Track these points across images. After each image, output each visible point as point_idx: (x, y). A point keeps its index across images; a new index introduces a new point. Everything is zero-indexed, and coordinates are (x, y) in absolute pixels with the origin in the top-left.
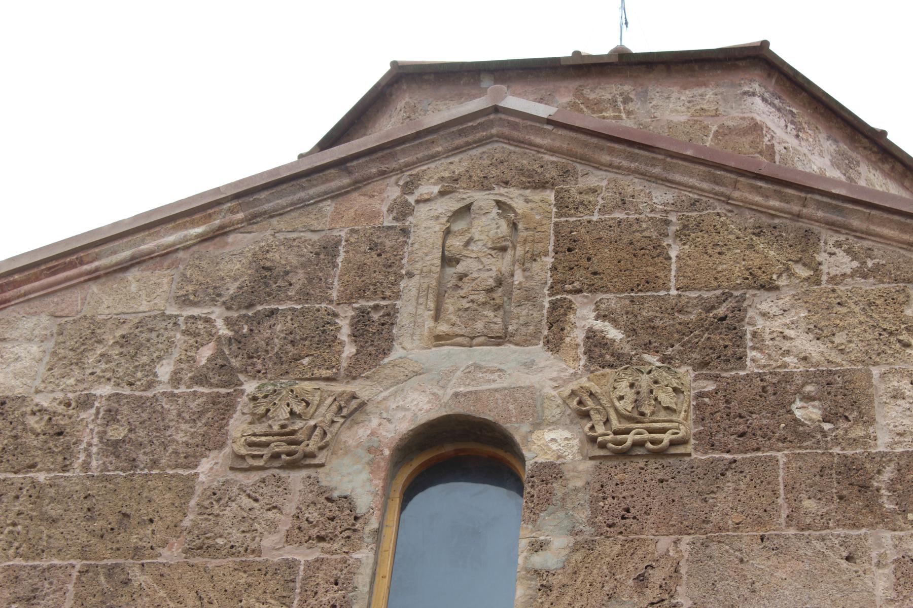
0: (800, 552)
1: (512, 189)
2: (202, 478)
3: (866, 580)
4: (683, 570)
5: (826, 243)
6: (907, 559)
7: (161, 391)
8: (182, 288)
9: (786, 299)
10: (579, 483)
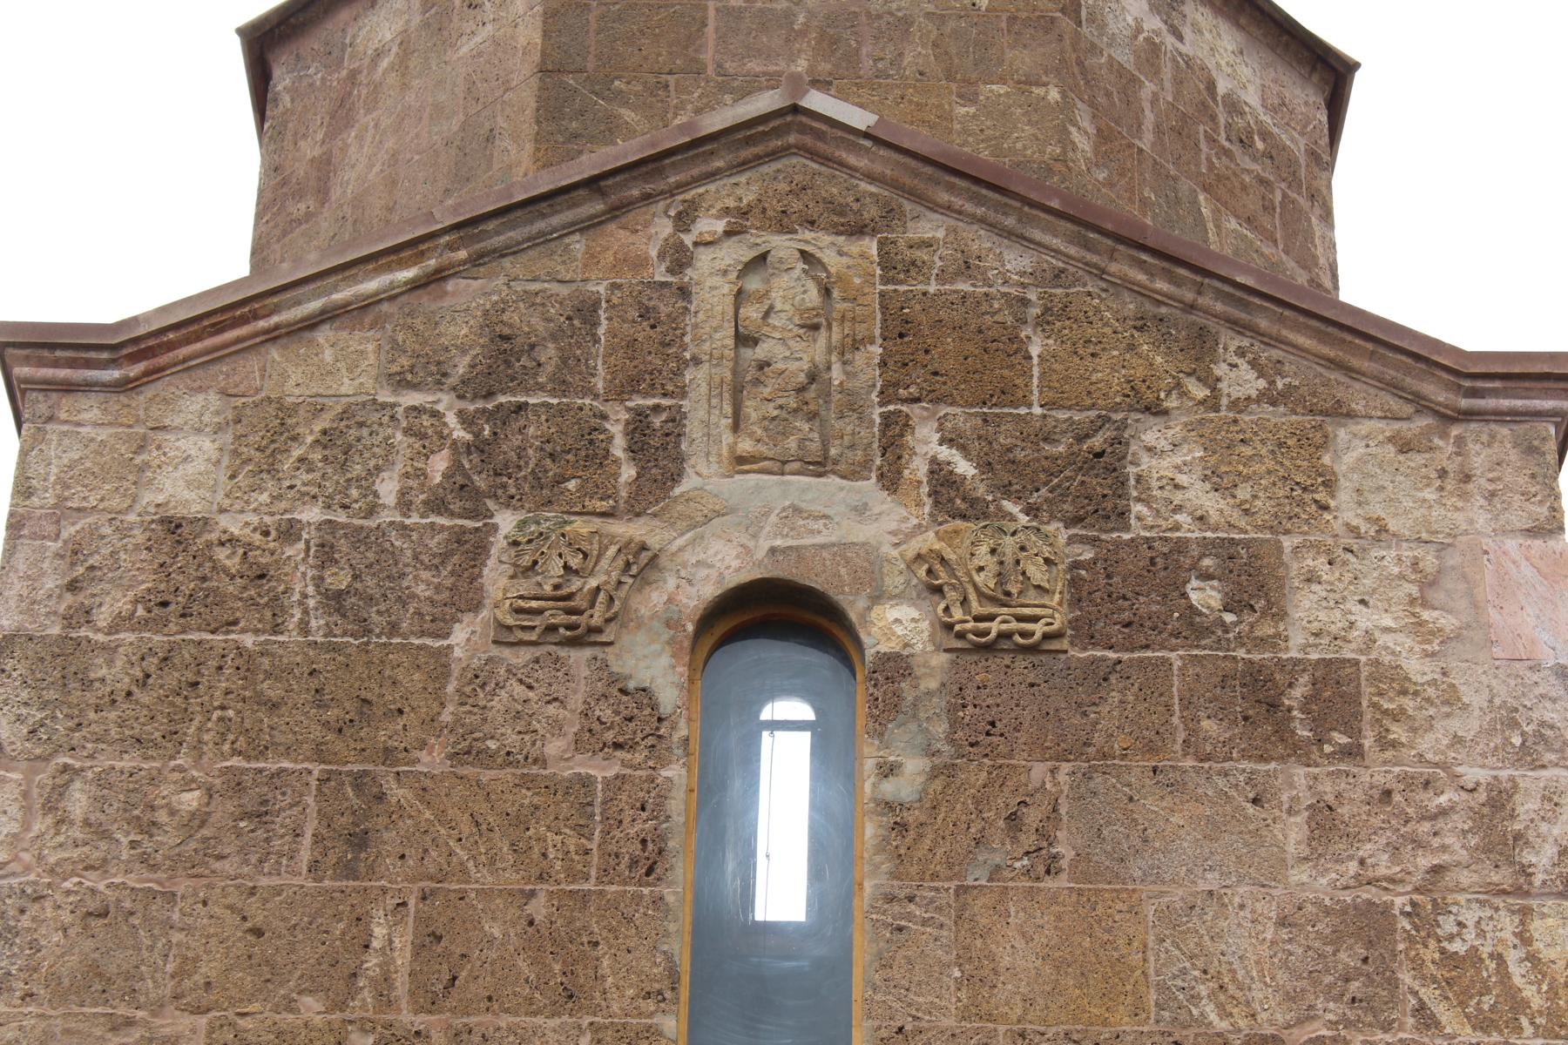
0: (1200, 791)
1: (820, 234)
2: (458, 653)
3: (1276, 832)
4: (1063, 811)
5: (1225, 349)
6: (1322, 804)
7: (388, 520)
8: (393, 361)
9: (1176, 431)
10: (933, 684)
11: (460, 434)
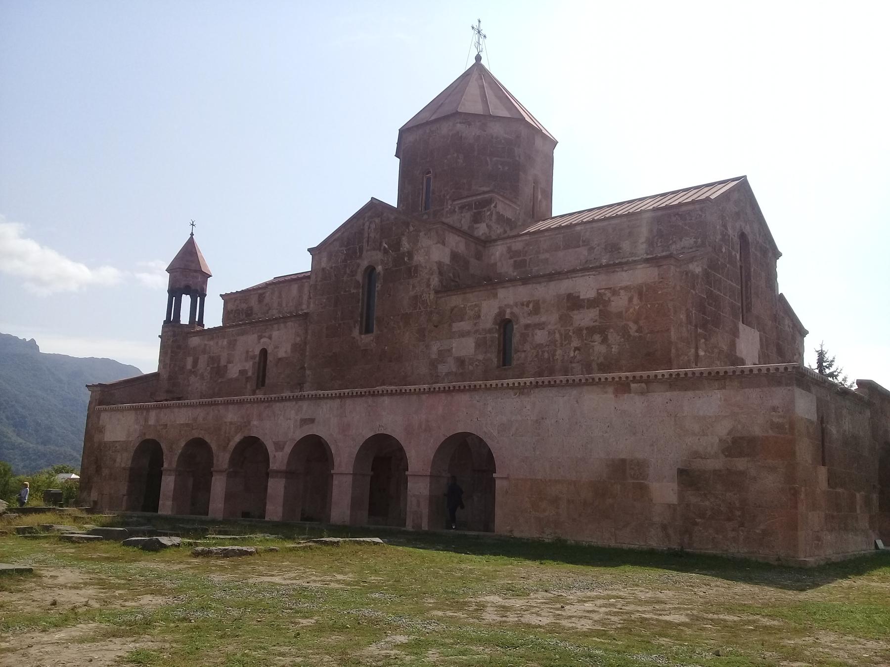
11: (345, 252)
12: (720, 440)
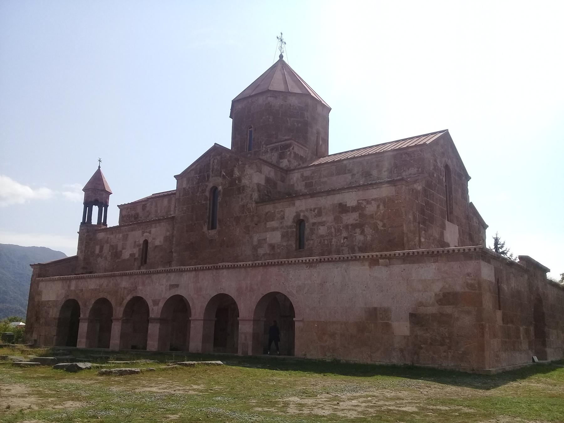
12: (436, 295)
